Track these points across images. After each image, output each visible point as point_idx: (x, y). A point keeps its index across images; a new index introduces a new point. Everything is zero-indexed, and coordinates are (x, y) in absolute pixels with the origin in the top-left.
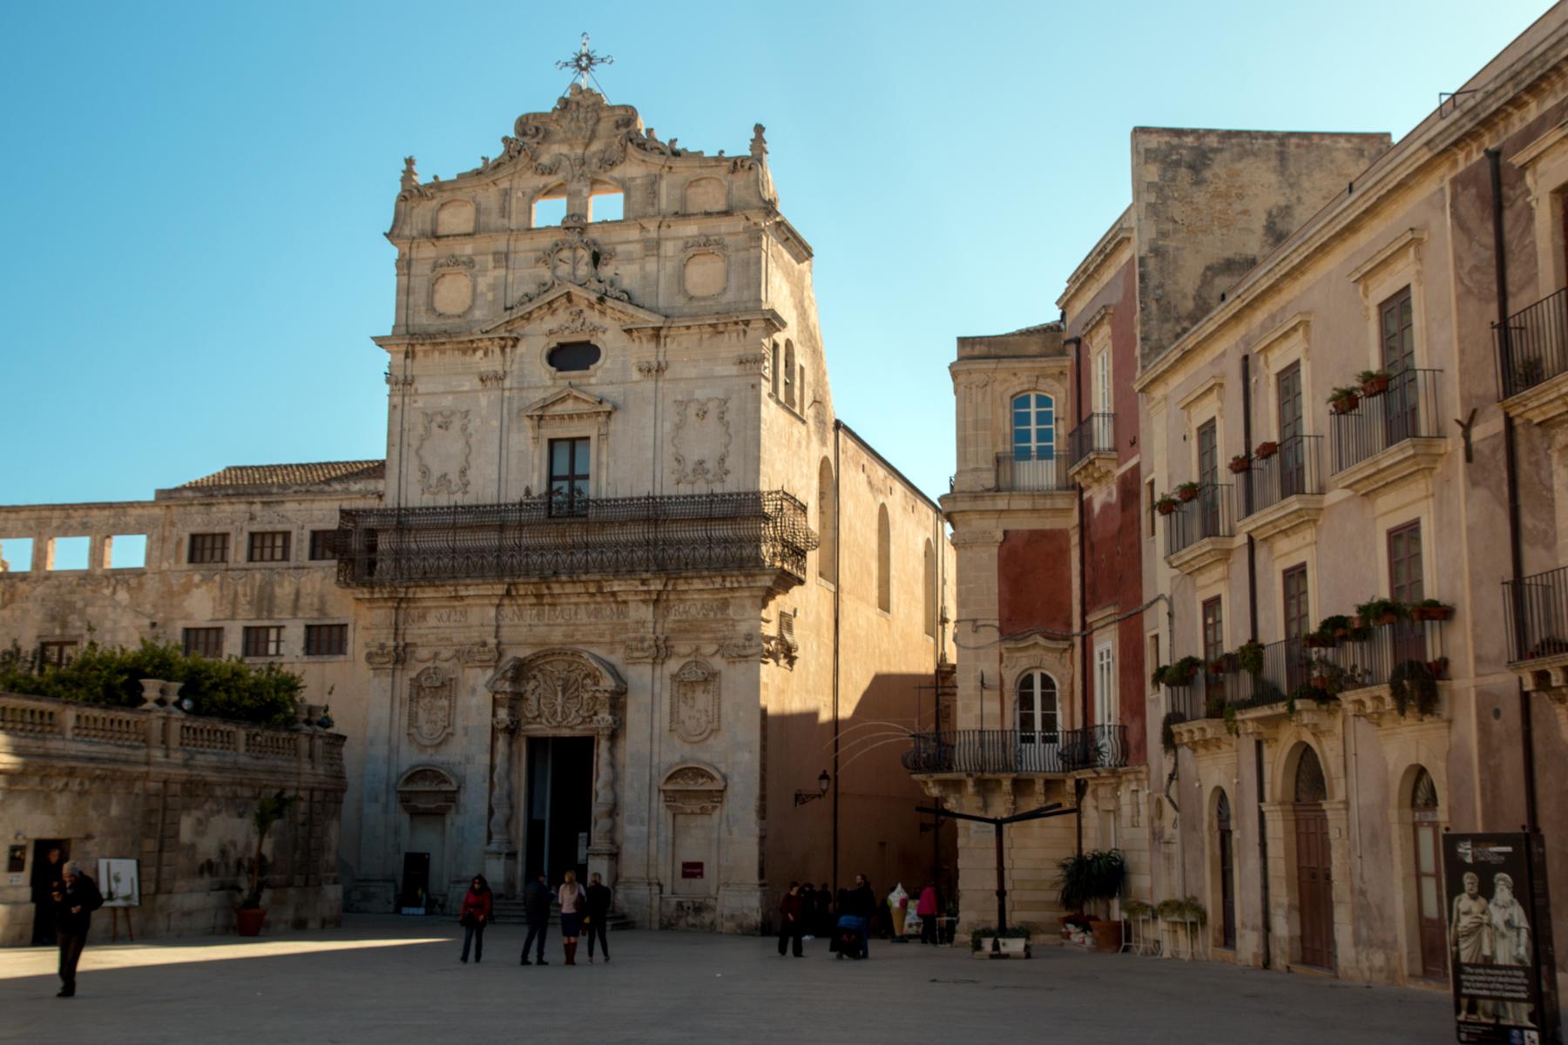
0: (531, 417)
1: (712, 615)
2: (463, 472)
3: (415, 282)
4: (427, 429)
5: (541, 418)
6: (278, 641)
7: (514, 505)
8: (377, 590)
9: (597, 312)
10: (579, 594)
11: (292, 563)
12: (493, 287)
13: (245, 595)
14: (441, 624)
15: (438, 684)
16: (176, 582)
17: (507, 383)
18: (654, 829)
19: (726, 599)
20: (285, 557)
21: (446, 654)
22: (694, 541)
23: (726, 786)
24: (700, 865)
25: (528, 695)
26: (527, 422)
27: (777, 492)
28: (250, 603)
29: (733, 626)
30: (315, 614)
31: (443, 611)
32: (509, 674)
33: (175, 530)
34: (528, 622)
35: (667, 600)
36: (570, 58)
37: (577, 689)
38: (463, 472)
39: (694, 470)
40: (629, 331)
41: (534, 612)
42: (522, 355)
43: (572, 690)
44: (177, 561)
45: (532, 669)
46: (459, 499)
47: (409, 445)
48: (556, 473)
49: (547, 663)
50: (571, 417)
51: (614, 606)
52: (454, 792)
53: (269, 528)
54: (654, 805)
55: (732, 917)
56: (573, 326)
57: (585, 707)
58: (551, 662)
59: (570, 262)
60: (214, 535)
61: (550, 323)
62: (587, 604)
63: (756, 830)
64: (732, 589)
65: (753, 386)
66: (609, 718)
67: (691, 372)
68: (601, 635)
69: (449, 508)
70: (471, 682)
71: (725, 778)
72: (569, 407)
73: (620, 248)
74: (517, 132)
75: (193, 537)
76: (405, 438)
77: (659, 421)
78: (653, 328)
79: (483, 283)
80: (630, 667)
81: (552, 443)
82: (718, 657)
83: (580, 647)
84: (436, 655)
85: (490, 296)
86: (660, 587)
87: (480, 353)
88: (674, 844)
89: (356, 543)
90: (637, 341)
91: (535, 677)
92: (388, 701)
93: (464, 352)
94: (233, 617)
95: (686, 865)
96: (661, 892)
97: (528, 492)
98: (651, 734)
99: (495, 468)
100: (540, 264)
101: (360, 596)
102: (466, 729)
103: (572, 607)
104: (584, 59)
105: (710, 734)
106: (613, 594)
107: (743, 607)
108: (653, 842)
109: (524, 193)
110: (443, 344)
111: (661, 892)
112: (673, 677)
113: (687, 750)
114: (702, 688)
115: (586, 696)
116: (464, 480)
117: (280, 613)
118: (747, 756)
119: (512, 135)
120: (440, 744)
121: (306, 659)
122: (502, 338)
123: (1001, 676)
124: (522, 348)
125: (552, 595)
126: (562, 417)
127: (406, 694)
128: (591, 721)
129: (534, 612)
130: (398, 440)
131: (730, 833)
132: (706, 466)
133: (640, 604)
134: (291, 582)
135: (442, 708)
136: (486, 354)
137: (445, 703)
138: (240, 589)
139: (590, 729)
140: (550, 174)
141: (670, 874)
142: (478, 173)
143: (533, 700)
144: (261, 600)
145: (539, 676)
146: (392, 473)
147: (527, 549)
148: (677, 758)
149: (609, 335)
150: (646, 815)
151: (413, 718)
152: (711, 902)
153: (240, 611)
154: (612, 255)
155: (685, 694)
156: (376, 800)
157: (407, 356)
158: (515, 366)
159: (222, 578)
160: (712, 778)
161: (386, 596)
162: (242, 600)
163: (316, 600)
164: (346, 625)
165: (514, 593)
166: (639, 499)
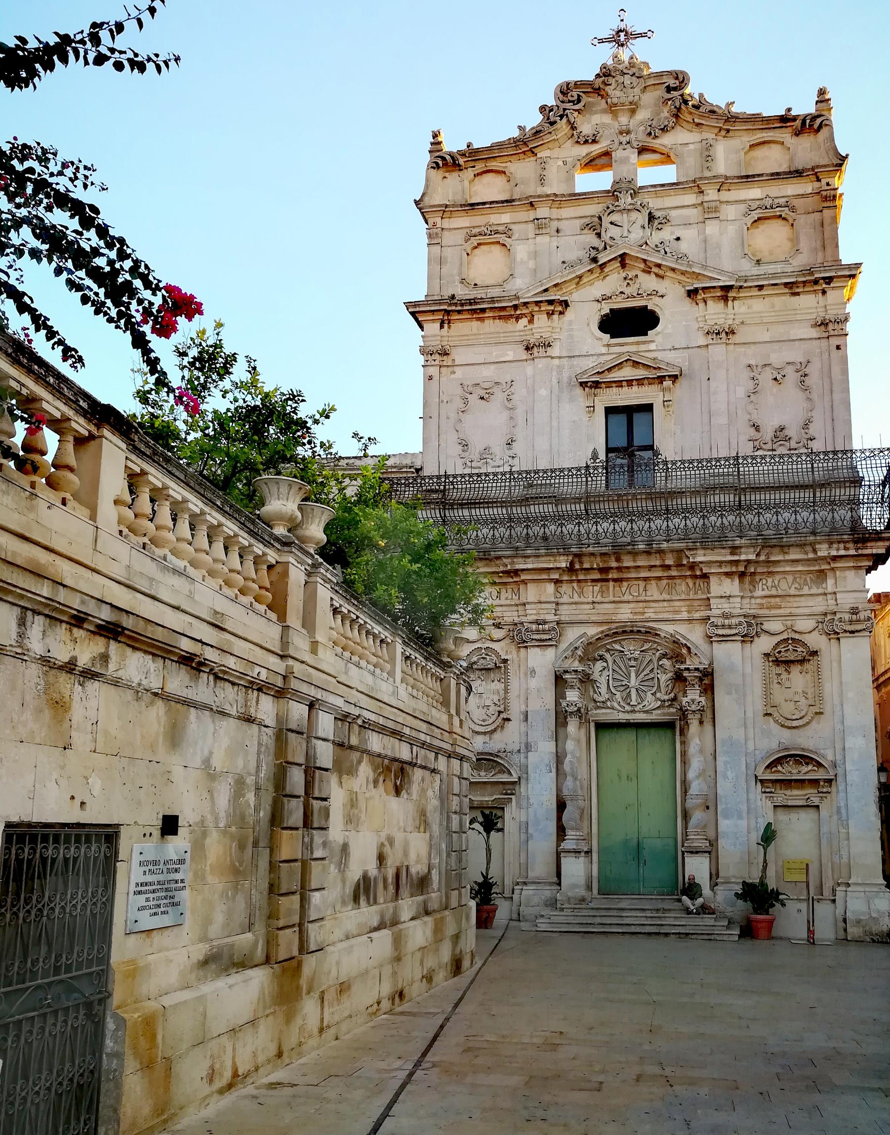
0: (583, 384)
3: (448, 252)
4: (466, 402)
5: (596, 385)
7: (579, 469)
9: (653, 276)
17: (555, 351)
25: (596, 676)
32: (579, 652)
34: (590, 600)
36: (607, 33)
40: (692, 294)
42: (570, 323)
43: (647, 671)
45: (598, 649)
49: (615, 642)
50: (630, 383)
51: (690, 582)
52: (514, 783)
54: (752, 796)
55: (859, 922)
56: (628, 291)
57: (663, 690)
65: (838, 347)
71: (835, 766)
72: (627, 373)
73: (673, 214)
74: (557, 98)
81: (610, 411)
85: (531, 264)
86: (752, 557)
87: (524, 321)
90: (702, 305)
91: (602, 658)
97: (595, 456)
100: (586, 231)
103: (642, 584)
104: (622, 34)
106: (692, 566)
109: (565, 163)
110: (483, 310)
116: (511, 453)
119: (551, 102)
124: (570, 314)
126: (619, 384)
129: (597, 589)
133: (723, 578)
139: (672, 714)
140: (594, 141)
142: (515, 143)
143: (603, 680)
145: (607, 656)
148: (774, 746)
150: (744, 808)
157: (442, 327)
158: (564, 335)
160: (819, 765)
165: (577, 566)
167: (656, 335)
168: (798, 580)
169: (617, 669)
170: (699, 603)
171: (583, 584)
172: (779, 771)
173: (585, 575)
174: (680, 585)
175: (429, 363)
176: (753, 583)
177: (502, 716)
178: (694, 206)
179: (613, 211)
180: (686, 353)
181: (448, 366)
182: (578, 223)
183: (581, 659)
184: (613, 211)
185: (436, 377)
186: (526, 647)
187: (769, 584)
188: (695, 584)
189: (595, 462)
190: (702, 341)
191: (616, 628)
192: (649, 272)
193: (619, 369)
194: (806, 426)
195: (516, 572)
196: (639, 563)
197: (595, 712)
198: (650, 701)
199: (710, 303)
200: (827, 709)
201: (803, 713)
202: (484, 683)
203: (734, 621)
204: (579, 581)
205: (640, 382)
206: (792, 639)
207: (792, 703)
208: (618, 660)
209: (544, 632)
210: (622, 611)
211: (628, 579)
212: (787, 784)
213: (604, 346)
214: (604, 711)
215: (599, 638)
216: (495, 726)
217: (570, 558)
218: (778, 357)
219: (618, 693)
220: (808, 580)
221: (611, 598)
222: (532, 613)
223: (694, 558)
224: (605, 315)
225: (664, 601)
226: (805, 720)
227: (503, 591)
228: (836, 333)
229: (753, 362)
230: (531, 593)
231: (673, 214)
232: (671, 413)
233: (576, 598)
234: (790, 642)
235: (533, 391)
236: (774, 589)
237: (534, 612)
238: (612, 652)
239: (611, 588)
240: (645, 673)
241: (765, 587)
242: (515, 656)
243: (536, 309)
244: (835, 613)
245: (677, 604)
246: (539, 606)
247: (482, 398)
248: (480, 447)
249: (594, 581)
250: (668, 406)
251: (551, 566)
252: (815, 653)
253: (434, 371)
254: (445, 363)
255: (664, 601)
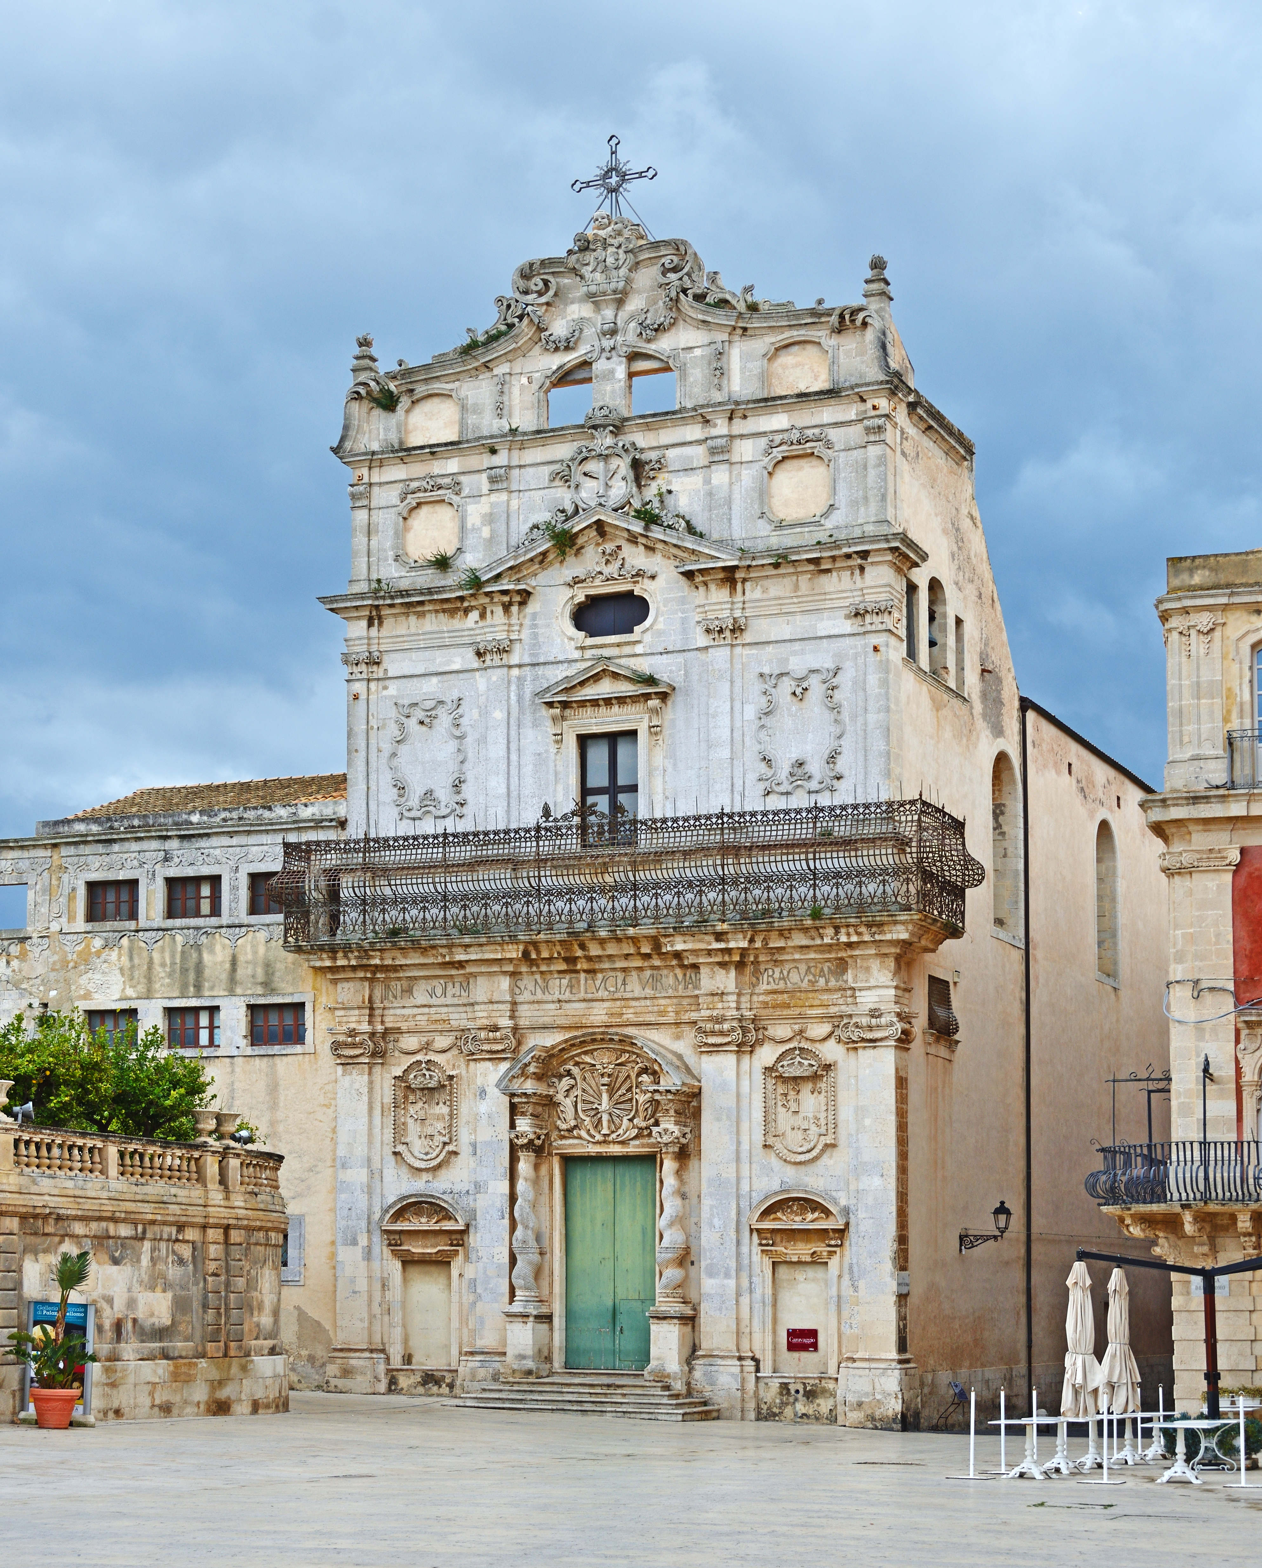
1: (822, 981)
2: (457, 786)
4: (402, 727)
6: (212, 1028)
8: (340, 955)
9: (642, 548)
10: (627, 956)
11: (225, 920)
12: (490, 519)
13: (163, 965)
14: (434, 1001)
15: (433, 1084)
16: (72, 949)
18: (745, 1283)
19: (842, 959)
20: (215, 911)
21: (442, 1042)
22: (791, 877)
23: (847, 1224)
24: (813, 1333)
26: (546, 713)
27: (912, 802)
28: (170, 975)
29: (853, 996)
30: (260, 990)
31: (435, 982)
33: (65, 877)
34: (557, 996)
35: (756, 963)
37: (629, 1089)
38: (457, 786)
39: (791, 774)
40: (689, 575)
41: (565, 982)
44: (71, 919)
45: (565, 1062)
46: (451, 825)
47: (379, 751)
48: (591, 783)
49: (586, 1053)
51: (679, 972)
53: (190, 872)
54: (745, 1249)
56: (608, 570)
57: (642, 1114)
58: (591, 1052)
59: (601, 478)
60: (117, 884)
61: (573, 568)
62: (640, 969)
63: (892, 1286)
64: (850, 945)
66: (676, 1129)
67: (782, 629)
68: (662, 1013)
69: (435, 837)
70: (479, 1081)
71: (846, 1211)
72: (605, 688)
75: (91, 886)
76: (372, 741)
77: (737, 705)
78: (724, 569)
79: (475, 512)
80: (705, 1057)
82: (832, 1042)
83: (630, 1031)
84: (426, 1047)
85: (486, 532)
88: (775, 1305)
89: (314, 892)
90: (702, 589)
92: (364, 1107)
93: (452, 612)
94: (148, 996)
95: (792, 1333)
96: (758, 1370)
98: (738, 1152)
99: (502, 779)
101: (318, 964)
102: (474, 1146)
103: (620, 975)
105: (823, 1151)
106: (678, 955)
107: (868, 969)
108: (745, 1300)
111: (758, 1370)
112: (768, 1070)
113: (790, 1175)
114: (810, 1085)
115: (642, 1098)
116: (458, 798)
117: (212, 988)
118: (877, 1181)
120: (439, 1166)
121: (249, 1051)
122: (505, 592)
123: (1237, 1062)
125: (589, 959)
126: (595, 703)
127: (388, 1099)
128: (650, 1135)
129: (565, 982)
130: (363, 744)
131: (856, 1289)
132: (808, 768)
133: (717, 968)
134: (224, 947)
135: (441, 1117)
136: (483, 616)
137: (445, 1110)
138: (156, 956)
141: (769, 1346)
143: (568, 1102)
144: (184, 971)
146: (357, 788)
147: (549, 892)
148: (776, 1187)
149: (660, 581)
150: (733, 1264)
151: (399, 1130)
152: (831, 1385)
153: (157, 986)
154: (660, 466)
155: (786, 1095)
156: (354, 1242)
158: (525, 635)
159: (130, 941)
160: (827, 1212)
161: (353, 962)
162: (157, 968)
163: (260, 972)
164: (302, 1005)
166: (708, 817)
167: (643, 632)
168: (813, 970)
169: (588, 1088)
170: (688, 1000)
171: (548, 976)
172: (780, 1219)
173: (548, 965)
174: (667, 977)
175: (353, 677)
176: (757, 973)
177: (447, 1148)
178: (699, 442)
179: (586, 458)
180: (680, 658)
181: (378, 679)
182: (546, 470)
183: (539, 1077)
184: (586, 458)
185: (363, 696)
186: (475, 1060)
187: (777, 975)
188: (685, 975)
189: (547, 821)
190: (702, 640)
191: (583, 1036)
192: (636, 543)
193: (595, 681)
194: (832, 759)
195: (461, 965)
196: (610, 952)
197: (560, 1142)
198: (627, 1130)
199: (713, 587)
200: (842, 1141)
201: (812, 1144)
202: (426, 1106)
203: (726, 1026)
204: (542, 973)
205: (621, 700)
206: (800, 1049)
207: (800, 1132)
208: (588, 1075)
209: (495, 1041)
210: (595, 1011)
211: (602, 970)
212: (792, 1234)
213: (577, 648)
214: (571, 1141)
215: (563, 1049)
216: (439, 1160)
217: (521, 947)
218: (798, 664)
219: (588, 1119)
220: (826, 969)
221: (582, 995)
222: (482, 1016)
223: (672, 946)
224: (579, 604)
225: (646, 998)
226: (814, 1153)
227: (450, 985)
228: (873, 628)
229: (766, 670)
230: (481, 989)
231: (671, 453)
232: (660, 742)
233: (539, 996)
234: (797, 1052)
235: (485, 713)
236: (782, 982)
237: (485, 1014)
238: (582, 1066)
239: (582, 982)
240: (620, 1093)
241: (771, 979)
242: (464, 1072)
243: (487, 600)
244: (850, 1016)
245: (663, 1002)
246: (491, 1007)
247: (422, 723)
248: (420, 791)
249: (560, 972)
250: (656, 734)
251: (499, 957)
252: (828, 1067)
253: (359, 687)
254: (375, 676)
255: (646, 998)
